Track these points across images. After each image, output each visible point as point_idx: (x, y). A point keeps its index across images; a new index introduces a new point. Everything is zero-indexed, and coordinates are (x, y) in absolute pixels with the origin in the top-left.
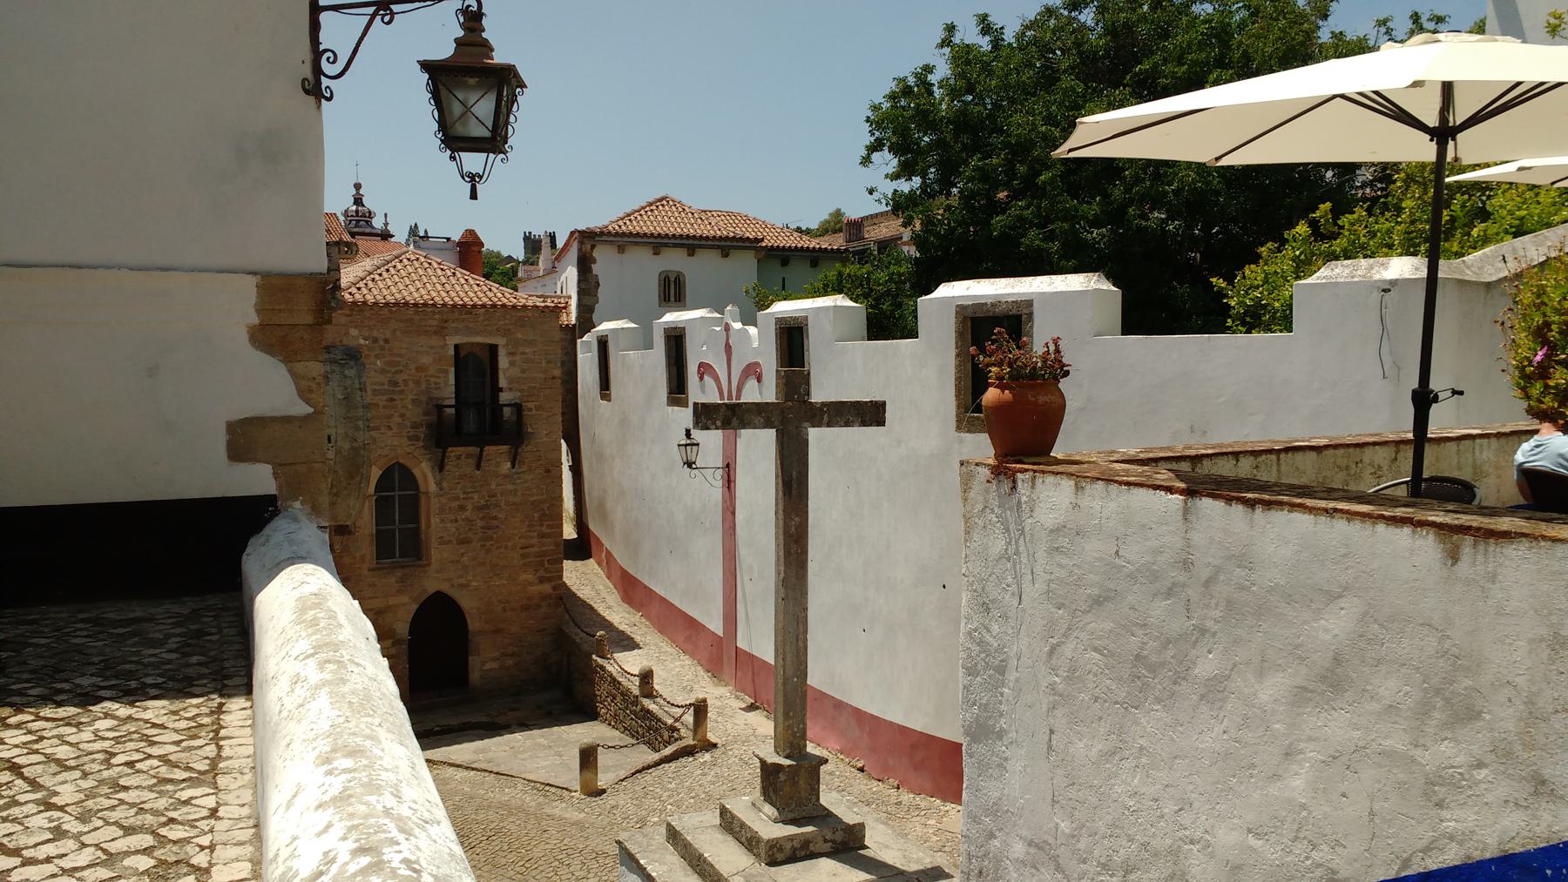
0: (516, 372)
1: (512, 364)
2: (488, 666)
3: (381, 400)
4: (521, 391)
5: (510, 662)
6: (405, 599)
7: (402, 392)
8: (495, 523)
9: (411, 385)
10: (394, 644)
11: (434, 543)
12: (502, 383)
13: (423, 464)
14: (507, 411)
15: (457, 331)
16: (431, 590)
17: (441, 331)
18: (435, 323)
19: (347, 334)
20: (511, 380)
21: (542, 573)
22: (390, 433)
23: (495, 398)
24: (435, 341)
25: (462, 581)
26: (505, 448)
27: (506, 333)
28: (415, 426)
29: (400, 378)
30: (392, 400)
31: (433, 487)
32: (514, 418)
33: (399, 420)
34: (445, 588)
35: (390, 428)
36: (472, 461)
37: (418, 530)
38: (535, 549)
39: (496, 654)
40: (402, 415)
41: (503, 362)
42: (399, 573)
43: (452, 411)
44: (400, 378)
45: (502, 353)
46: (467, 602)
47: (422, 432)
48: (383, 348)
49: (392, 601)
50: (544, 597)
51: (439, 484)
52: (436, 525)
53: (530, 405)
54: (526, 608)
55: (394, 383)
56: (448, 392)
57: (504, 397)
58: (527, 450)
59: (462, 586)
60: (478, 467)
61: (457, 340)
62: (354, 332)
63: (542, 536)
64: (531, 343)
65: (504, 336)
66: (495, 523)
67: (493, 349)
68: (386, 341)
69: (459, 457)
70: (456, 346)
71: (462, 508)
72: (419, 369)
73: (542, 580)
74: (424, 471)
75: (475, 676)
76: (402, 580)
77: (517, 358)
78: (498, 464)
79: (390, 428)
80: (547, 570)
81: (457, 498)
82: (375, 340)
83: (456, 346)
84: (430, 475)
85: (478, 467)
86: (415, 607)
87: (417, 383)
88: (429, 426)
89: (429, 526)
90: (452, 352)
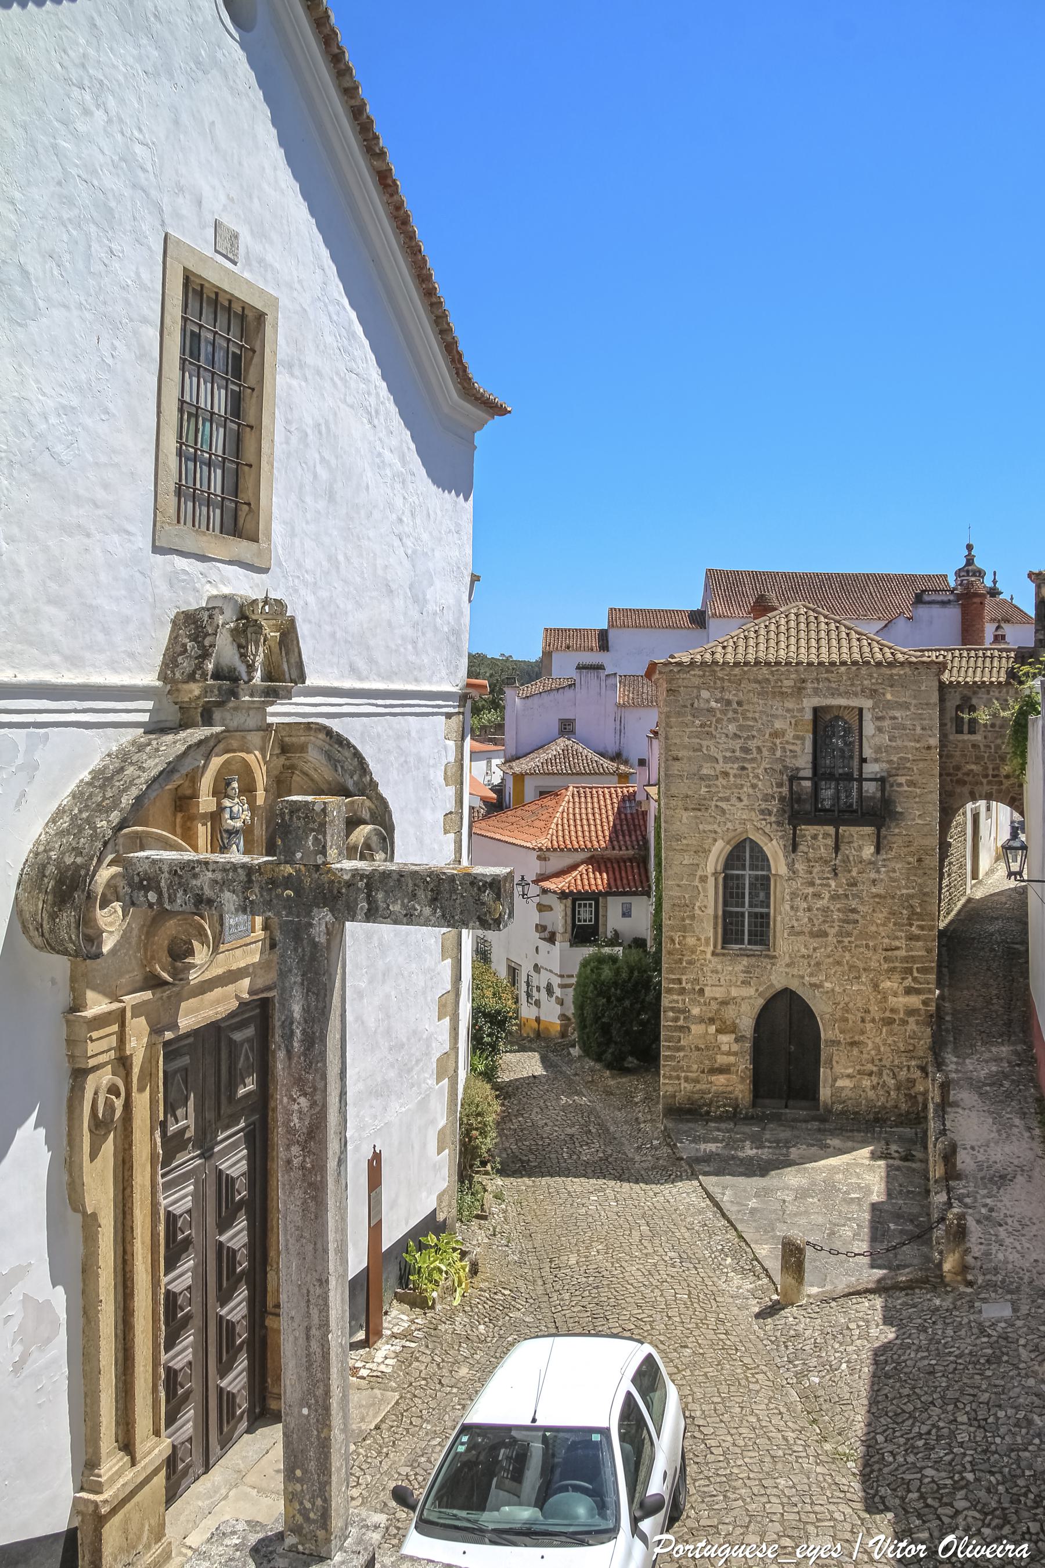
1: (880, 729)
2: (840, 1083)
3: (733, 768)
4: (890, 762)
5: (866, 1083)
6: (751, 991)
7: (753, 760)
8: (856, 916)
9: (765, 753)
10: (737, 1040)
12: (867, 753)
13: (774, 842)
15: (816, 692)
16: (779, 986)
17: (799, 690)
18: (791, 683)
19: (698, 697)
20: (878, 749)
21: (909, 982)
22: (740, 805)
24: (790, 704)
25: (814, 980)
26: (869, 830)
27: (873, 693)
28: (767, 798)
29: (752, 744)
30: (743, 768)
32: (879, 794)
33: (751, 791)
34: (794, 985)
35: (740, 799)
36: (830, 842)
37: (768, 915)
38: (902, 953)
39: (850, 1071)
40: (754, 786)
41: (869, 728)
42: (745, 961)
44: (752, 744)
45: (867, 716)
46: (820, 1006)
47: (774, 805)
48: (735, 712)
50: (911, 1012)
51: (791, 866)
52: (785, 912)
53: (902, 780)
54: (889, 1022)
55: (746, 750)
56: (804, 762)
58: (896, 833)
59: (813, 986)
60: (837, 849)
61: (817, 701)
62: (705, 694)
63: (911, 938)
64: (906, 706)
65: (871, 697)
66: (856, 916)
68: (739, 704)
69: (815, 837)
70: (816, 710)
71: (817, 896)
72: (775, 734)
73: (909, 991)
74: (774, 849)
77: (886, 723)
78: (860, 848)
79: (740, 799)
80: (915, 979)
81: (812, 884)
82: (729, 703)
83: (816, 710)
84: (781, 854)
85: (837, 849)
86: (761, 1002)
87: (773, 750)
88: (782, 799)
90: (809, 716)
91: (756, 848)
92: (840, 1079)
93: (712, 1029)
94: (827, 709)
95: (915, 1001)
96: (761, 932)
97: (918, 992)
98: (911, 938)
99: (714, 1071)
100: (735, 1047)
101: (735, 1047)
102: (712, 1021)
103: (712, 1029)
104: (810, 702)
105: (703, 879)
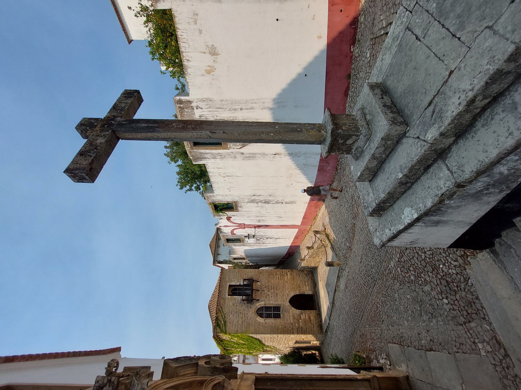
0: (236, 281)
1: (234, 281)
5: (307, 283)
11: (277, 303)
14: (245, 283)
16: (289, 304)
23: (242, 286)
26: (254, 284)
31: (263, 303)
34: (288, 300)
40: (245, 310)
41: (233, 283)
43: (244, 297)
46: (292, 294)
47: (249, 305)
49: (291, 314)
50: (291, 274)
52: (272, 302)
54: (294, 279)
55: (236, 312)
57: (242, 284)
58: (255, 278)
59: (288, 295)
60: (258, 291)
63: (276, 274)
67: (230, 286)
71: (268, 295)
72: (233, 305)
73: (287, 275)
75: (310, 293)
76: (286, 312)
85: (258, 291)
86: (293, 308)
89: (272, 304)
90: (230, 297)
91: (259, 309)
92: (307, 290)
93: (300, 321)
94: (228, 293)
95: (289, 274)
96: (277, 308)
97: (287, 273)
98: (276, 274)
99: (310, 321)
100: (304, 314)
101: (304, 314)
102: (299, 321)
103: (300, 321)
104: (227, 296)
105: (266, 323)
